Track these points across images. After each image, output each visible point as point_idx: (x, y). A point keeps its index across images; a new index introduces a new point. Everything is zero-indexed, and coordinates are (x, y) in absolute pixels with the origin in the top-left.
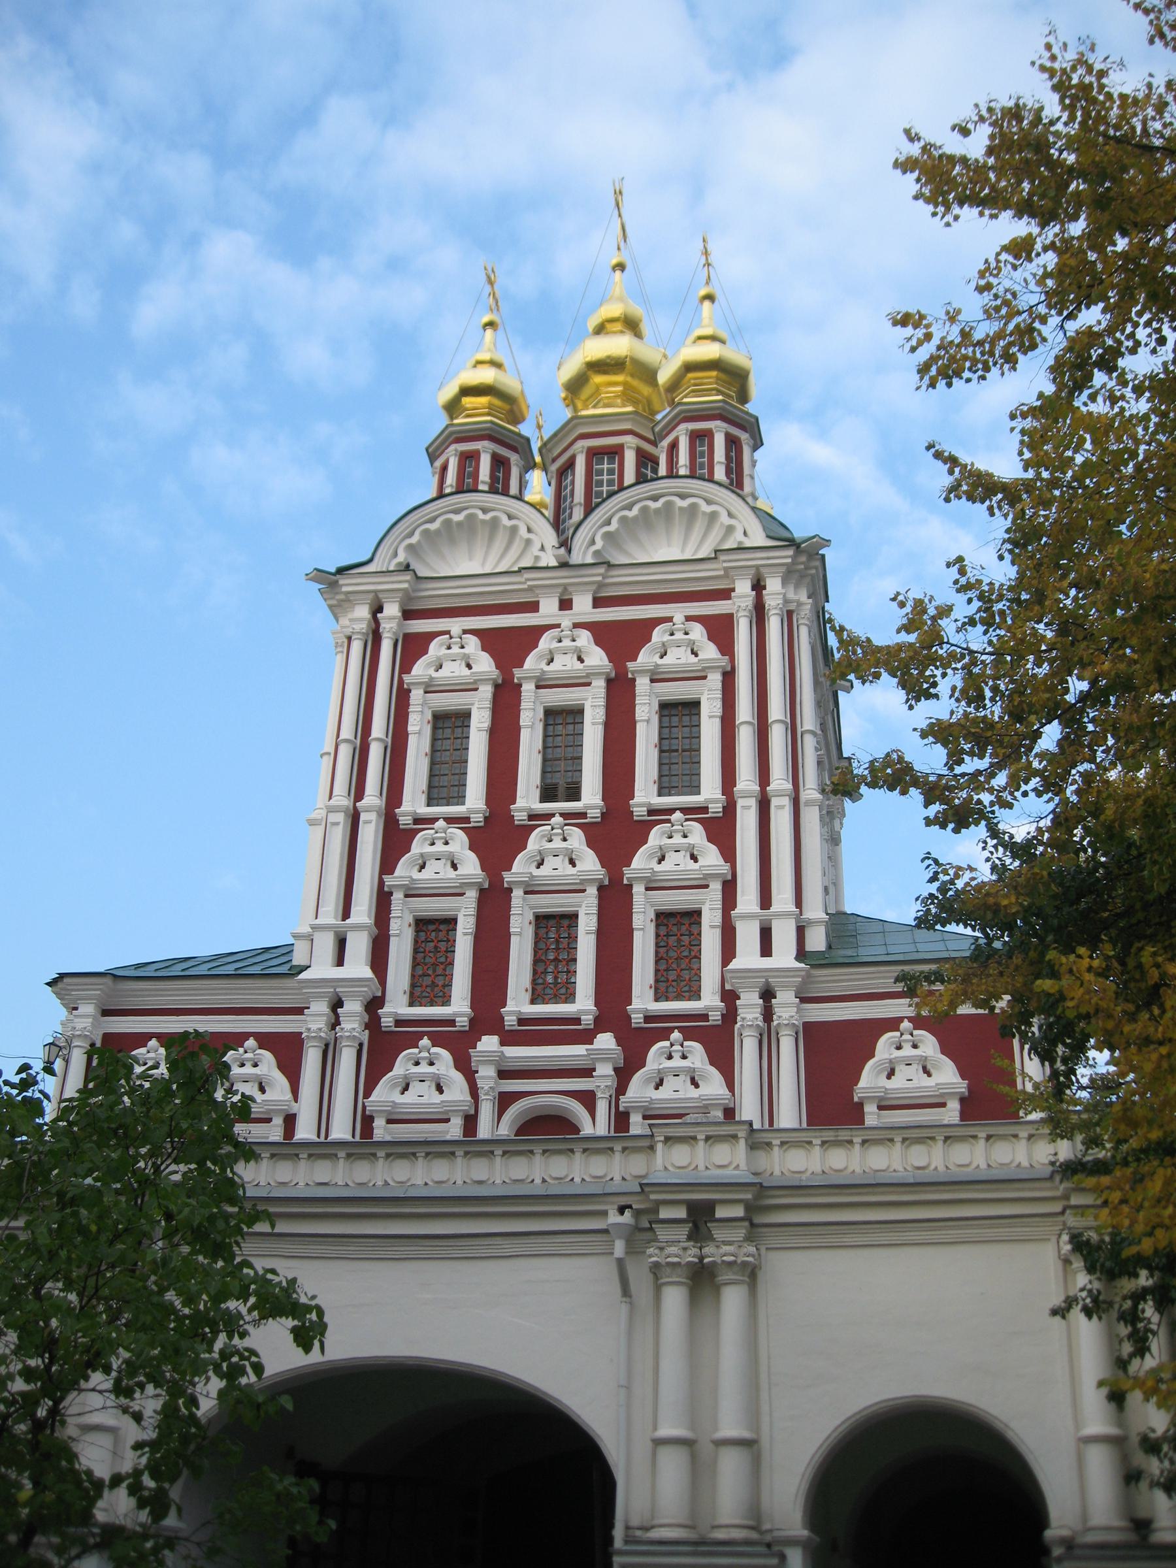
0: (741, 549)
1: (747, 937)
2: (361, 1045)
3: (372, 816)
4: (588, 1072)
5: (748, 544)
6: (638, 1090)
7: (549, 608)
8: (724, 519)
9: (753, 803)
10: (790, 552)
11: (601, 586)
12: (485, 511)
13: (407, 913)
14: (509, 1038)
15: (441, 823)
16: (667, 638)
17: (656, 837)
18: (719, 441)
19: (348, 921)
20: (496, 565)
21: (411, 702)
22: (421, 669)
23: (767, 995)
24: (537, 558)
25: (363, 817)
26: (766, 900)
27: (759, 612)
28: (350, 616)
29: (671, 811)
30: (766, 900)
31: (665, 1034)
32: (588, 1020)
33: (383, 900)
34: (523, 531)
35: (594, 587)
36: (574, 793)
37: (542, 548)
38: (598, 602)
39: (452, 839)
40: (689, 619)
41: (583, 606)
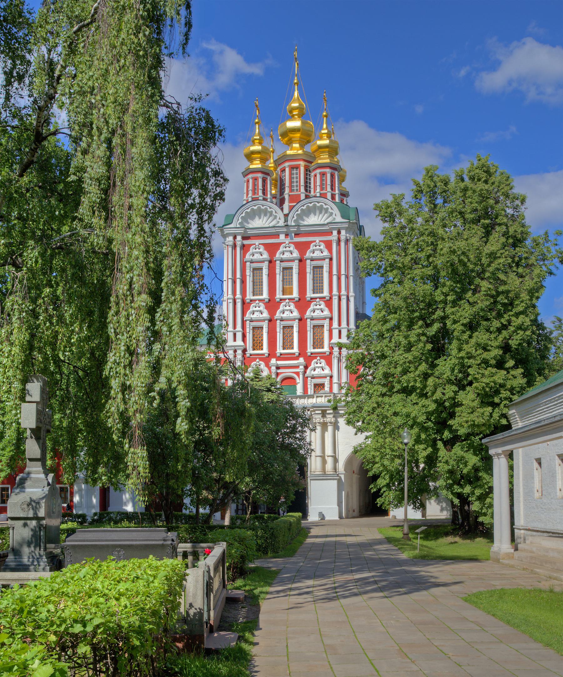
1: (335, 333)
4: (297, 367)
7: (282, 237)
8: (330, 210)
9: (337, 297)
12: (263, 206)
14: (279, 359)
17: (312, 307)
18: (329, 176)
22: (248, 257)
26: (340, 324)
29: (316, 298)
30: (340, 324)
31: (316, 358)
32: (297, 354)
34: (274, 213)
36: (291, 293)
40: (320, 241)
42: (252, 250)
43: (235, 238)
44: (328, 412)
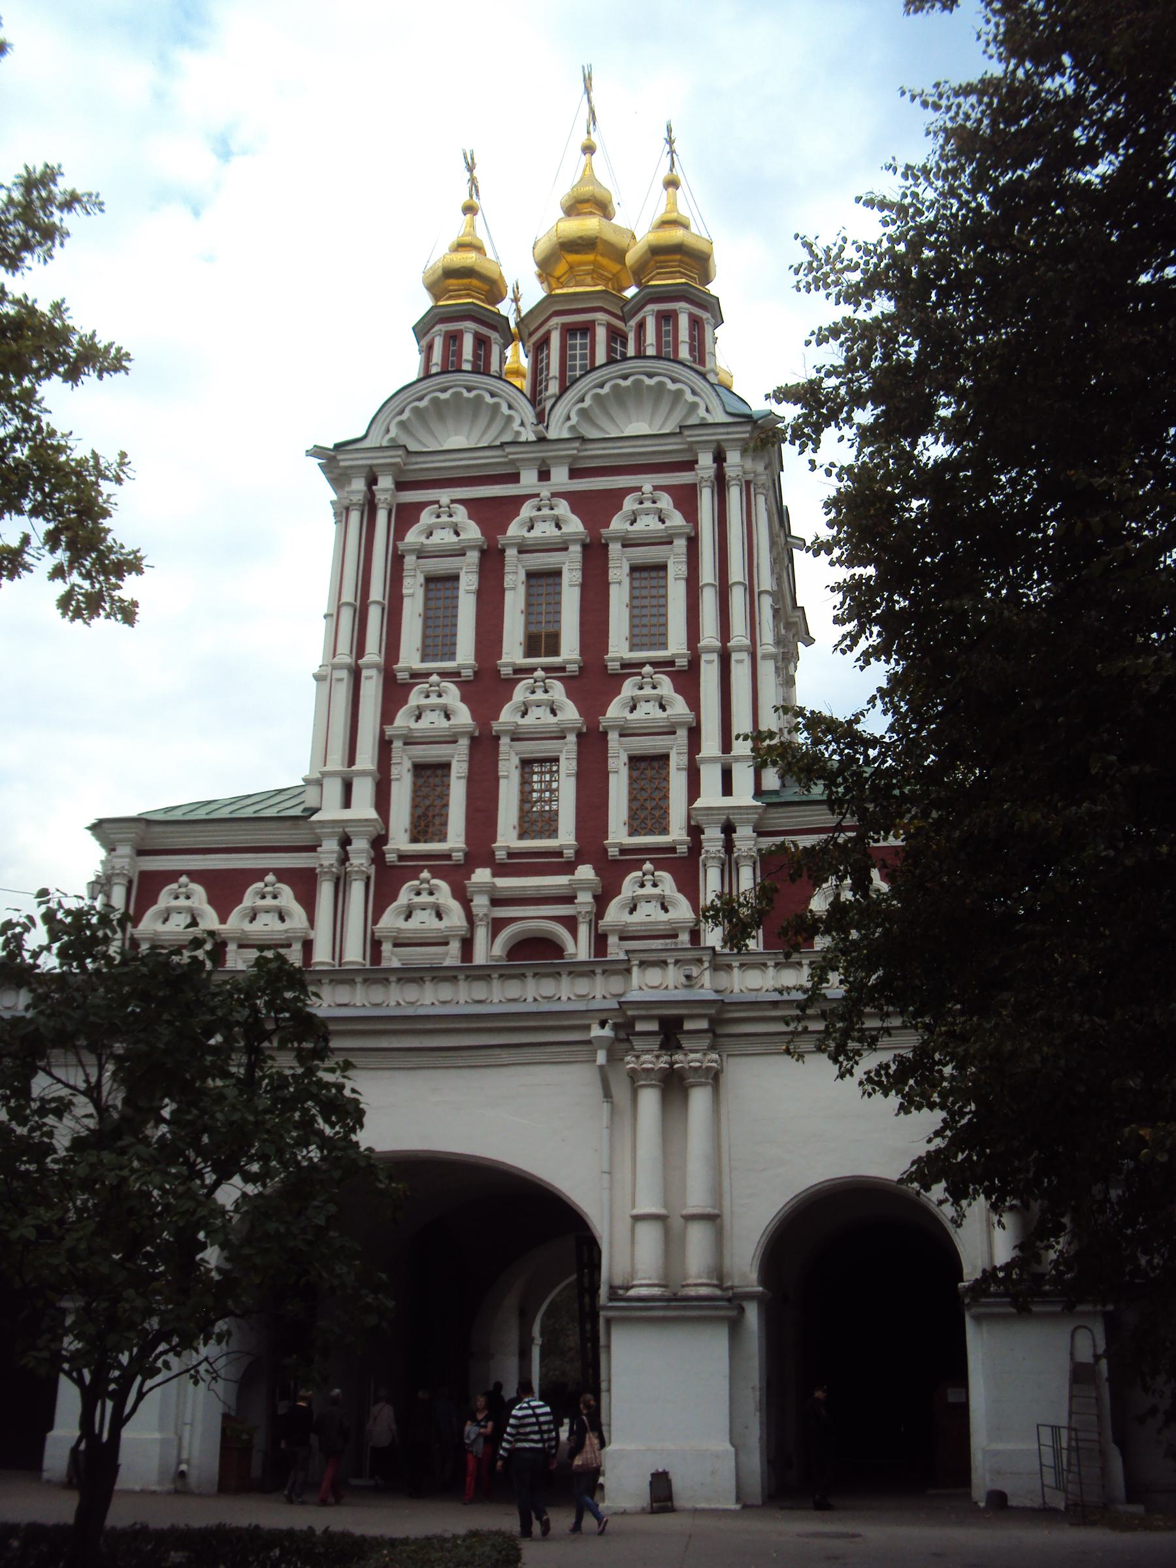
0: (704, 425)
1: (710, 778)
2: (368, 878)
3: (373, 672)
5: (710, 420)
6: (615, 914)
7: (529, 479)
10: (748, 428)
11: (575, 458)
12: (469, 389)
13: (405, 758)
14: (500, 870)
15: (435, 678)
16: (637, 506)
17: (628, 689)
18: (683, 321)
19: (353, 768)
20: (479, 441)
21: (405, 567)
22: (413, 537)
23: (728, 829)
24: (518, 433)
25: (365, 673)
27: (721, 484)
28: (347, 489)
29: (642, 665)
32: (569, 853)
33: (385, 746)
34: (504, 409)
35: (570, 460)
36: (554, 650)
37: (522, 424)
38: (574, 473)
39: (446, 693)
41: (560, 476)
42: (426, 517)
43: (372, 481)
44: (688, 1026)
